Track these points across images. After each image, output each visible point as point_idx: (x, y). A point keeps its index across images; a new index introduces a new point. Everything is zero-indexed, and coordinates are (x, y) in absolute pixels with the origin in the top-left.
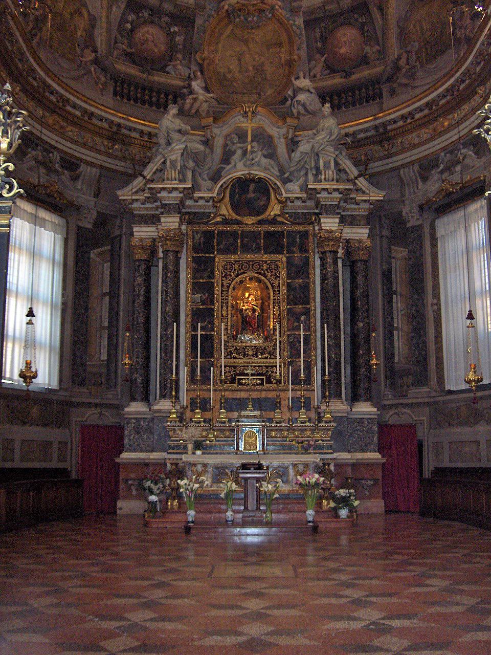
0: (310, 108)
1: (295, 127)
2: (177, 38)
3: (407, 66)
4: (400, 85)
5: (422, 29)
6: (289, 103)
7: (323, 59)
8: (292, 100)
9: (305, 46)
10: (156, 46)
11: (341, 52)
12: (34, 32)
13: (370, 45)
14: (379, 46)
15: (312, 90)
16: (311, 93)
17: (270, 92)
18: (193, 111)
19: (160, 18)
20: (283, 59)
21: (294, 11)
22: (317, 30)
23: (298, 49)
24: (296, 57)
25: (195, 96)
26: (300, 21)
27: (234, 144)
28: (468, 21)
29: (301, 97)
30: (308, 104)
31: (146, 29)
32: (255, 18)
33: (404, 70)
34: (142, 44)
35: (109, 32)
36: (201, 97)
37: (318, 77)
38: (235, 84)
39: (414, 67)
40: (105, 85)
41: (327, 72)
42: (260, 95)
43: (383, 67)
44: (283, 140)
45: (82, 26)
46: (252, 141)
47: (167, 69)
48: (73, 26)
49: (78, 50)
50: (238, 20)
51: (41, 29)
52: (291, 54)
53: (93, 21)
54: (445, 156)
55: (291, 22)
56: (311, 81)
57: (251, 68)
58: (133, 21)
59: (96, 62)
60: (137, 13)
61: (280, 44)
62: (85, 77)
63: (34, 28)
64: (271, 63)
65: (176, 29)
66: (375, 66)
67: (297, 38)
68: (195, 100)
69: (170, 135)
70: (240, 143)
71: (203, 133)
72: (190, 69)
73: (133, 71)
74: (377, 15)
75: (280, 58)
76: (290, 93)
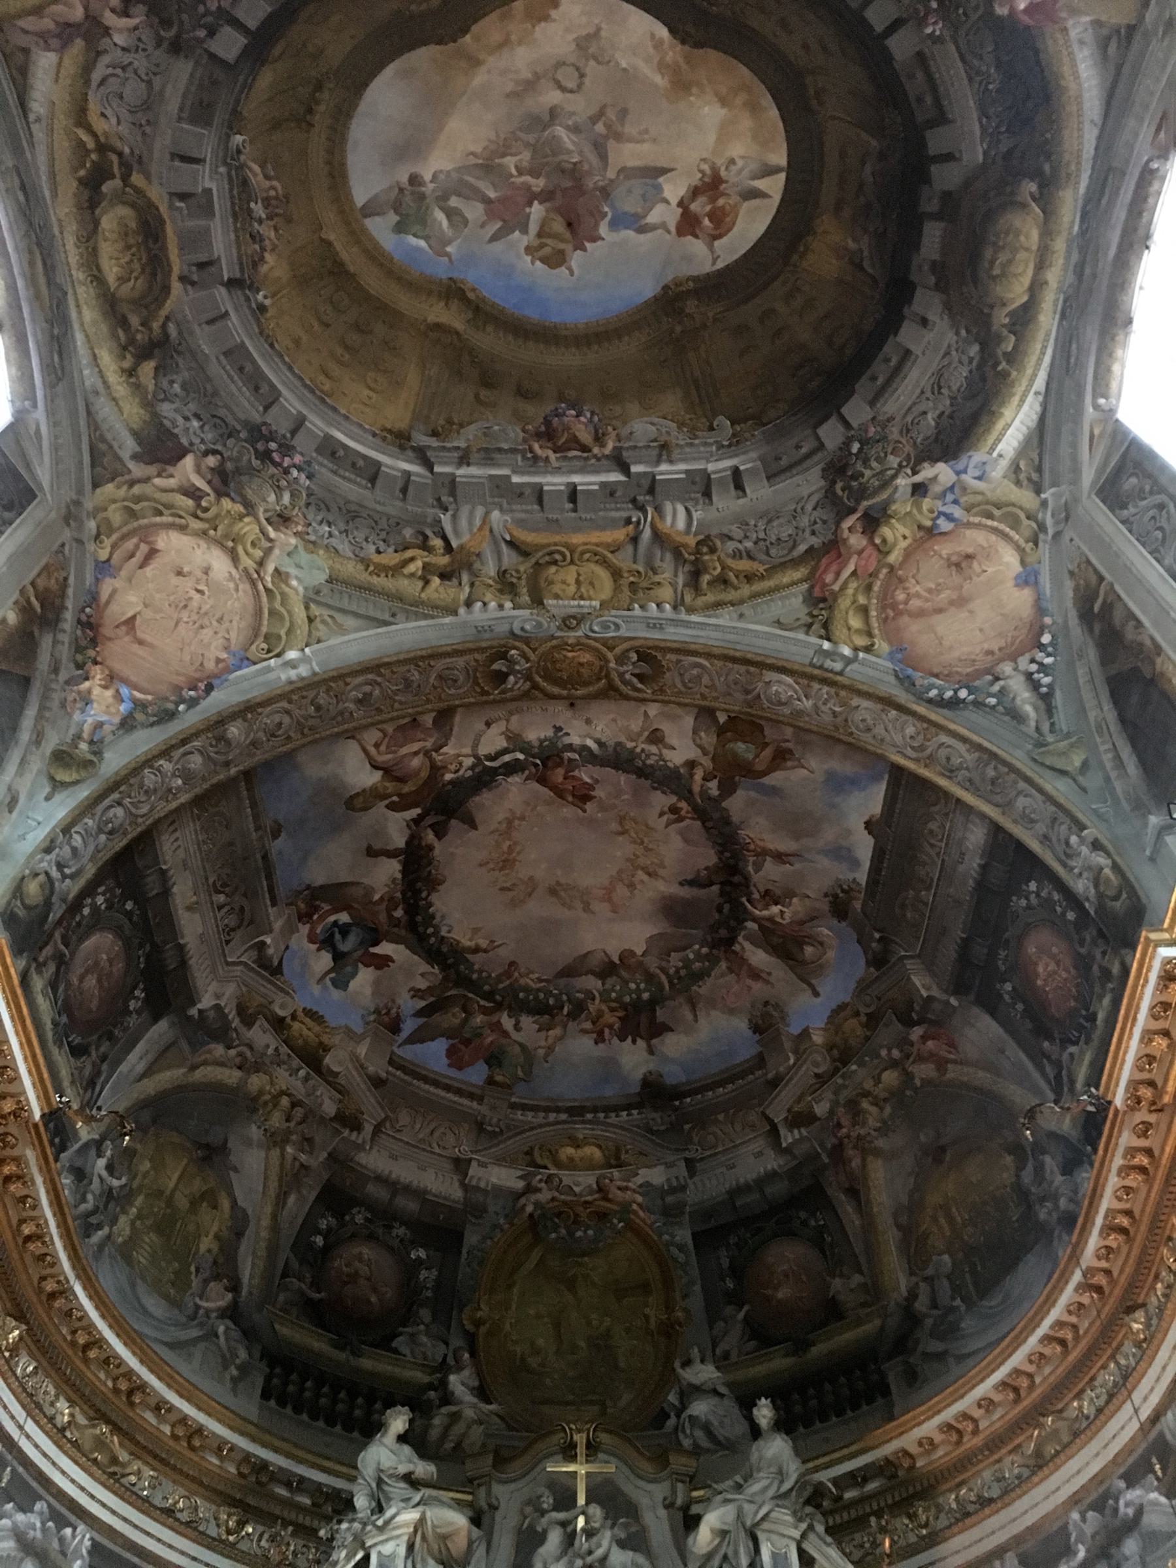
0: (721, 1433)
1: (692, 1478)
2: (424, 1274)
3: (935, 1312)
4: (928, 1357)
5: (951, 1219)
6: (672, 1421)
7: (741, 1315)
8: (678, 1416)
9: (697, 1288)
10: (375, 1290)
11: (780, 1295)
12: (93, 1220)
13: (841, 1276)
14: (860, 1272)
15: (723, 1390)
16: (722, 1396)
17: (626, 1398)
18: (449, 1445)
19: (389, 1227)
20: (653, 1320)
21: (671, 1213)
22: (723, 1252)
23: (685, 1296)
24: (680, 1314)
25: (453, 1409)
26: (684, 1235)
27: (543, 1513)
28: (1059, 1179)
29: (700, 1408)
30: (716, 1423)
31: (355, 1251)
32: (590, 1232)
33: (929, 1322)
34: (346, 1283)
35: (273, 1249)
36: (469, 1413)
37: (734, 1358)
38: (548, 1381)
39: (952, 1310)
40: (244, 1369)
41: (753, 1343)
42: (603, 1404)
43: (877, 1322)
44: (662, 1513)
45: (215, 1229)
46: (588, 1502)
47: (394, 1345)
48: (191, 1228)
49: (195, 1282)
50: (553, 1235)
51: (114, 1221)
52: (669, 1307)
53: (239, 1224)
54: (1084, 1519)
55: (666, 1237)
56: (718, 1368)
57: (582, 1344)
58: (329, 1229)
59: (232, 1313)
60: (340, 1215)
61: (645, 1288)
62: (202, 1345)
63: (95, 1211)
64: (628, 1331)
65: (422, 1254)
66: (859, 1322)
67: (680, 1272)
68: (455, 1417)
69: (386, 1488)
70: (556, 1508)
71: (469, 1498)
72: (447, 1344)
73: (317, 1343)
74: (847, 1209)
75: (647, 1317)
76: (672, 1398)
